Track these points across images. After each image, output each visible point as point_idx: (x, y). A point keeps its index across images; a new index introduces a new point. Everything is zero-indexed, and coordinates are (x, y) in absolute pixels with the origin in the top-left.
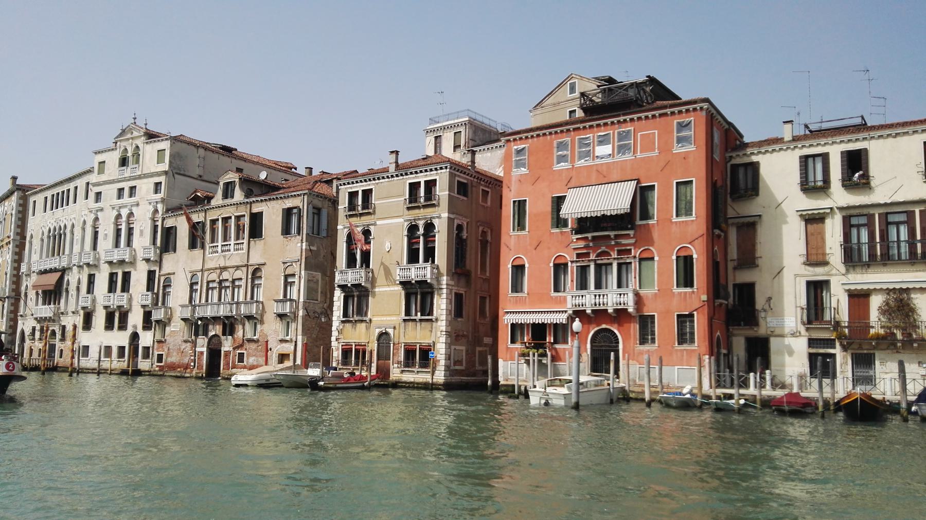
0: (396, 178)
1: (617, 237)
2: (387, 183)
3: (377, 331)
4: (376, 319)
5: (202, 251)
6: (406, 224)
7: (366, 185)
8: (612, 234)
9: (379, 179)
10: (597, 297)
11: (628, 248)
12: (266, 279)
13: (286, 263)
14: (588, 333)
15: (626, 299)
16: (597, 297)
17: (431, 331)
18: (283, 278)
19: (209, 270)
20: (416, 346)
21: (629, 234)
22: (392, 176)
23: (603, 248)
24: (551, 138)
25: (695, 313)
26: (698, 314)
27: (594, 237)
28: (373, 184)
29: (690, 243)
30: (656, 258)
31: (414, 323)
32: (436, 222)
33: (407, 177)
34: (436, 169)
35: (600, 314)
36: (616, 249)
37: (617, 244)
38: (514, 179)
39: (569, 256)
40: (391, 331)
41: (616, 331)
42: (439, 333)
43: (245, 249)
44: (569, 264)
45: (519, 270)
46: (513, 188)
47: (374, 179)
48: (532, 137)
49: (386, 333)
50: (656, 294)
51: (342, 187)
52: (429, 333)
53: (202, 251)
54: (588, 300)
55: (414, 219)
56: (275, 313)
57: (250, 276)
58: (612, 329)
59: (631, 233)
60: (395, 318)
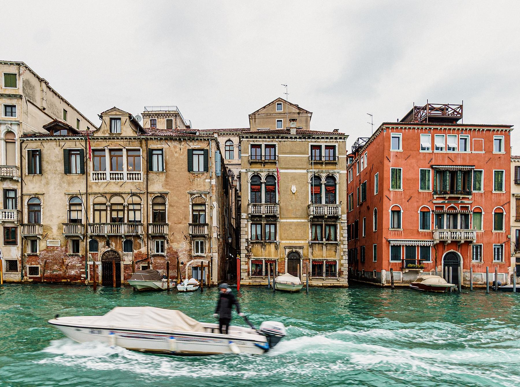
0: (298, 140)
1: (463, 198)
2: (291, 143)
3: (288, 250)
4: (285, 242)
5: (85, 176)
6: (310, 175)
7: (269, 141)
8: (461, 196)
9: (282, 138)
10: (452, 233)
11: (467, 206)
12: (170, 206)
13: (194, 194)
14: (443, 254)
15: (472, 235)
16: (452, 233)
17: (336, 252)
18: (191, 206)
19: (95, 194)
20: (323, 261)
21: (469, 198)
22: (296, 138)
23: (452, 205)
24: (418, 132)
25: (504, 244)
26: (505, 245)
27: (450, 198)
28: (277, 142)
29: (502, 206)
30: (483, 213)
31: (320, 245)
32: (337, 176)
33: (309, 140)
34: (336, 138)
35: (456, 243)
36: (460, 206)
37: (462, 203)
38: (392, 154)
39: (431, 208)
40: (301, 251)
41: (459, 254)
42: (342, 253)
43: (142, 179)
44: (431, 212)
45: (396, 212)
46: (391, 160)
47: (278, 138)
48: (405, 128)
49: (297, 252)
50: (483, 233)
51: (244, 139)
52: (334, 253)
53: (85, 176)
54: (447, 235)
55: (318, 172)
56: (190, 235)
57: (150, 203)
58: (457, 252)
59: (470, 197)
60: (303, 242)
